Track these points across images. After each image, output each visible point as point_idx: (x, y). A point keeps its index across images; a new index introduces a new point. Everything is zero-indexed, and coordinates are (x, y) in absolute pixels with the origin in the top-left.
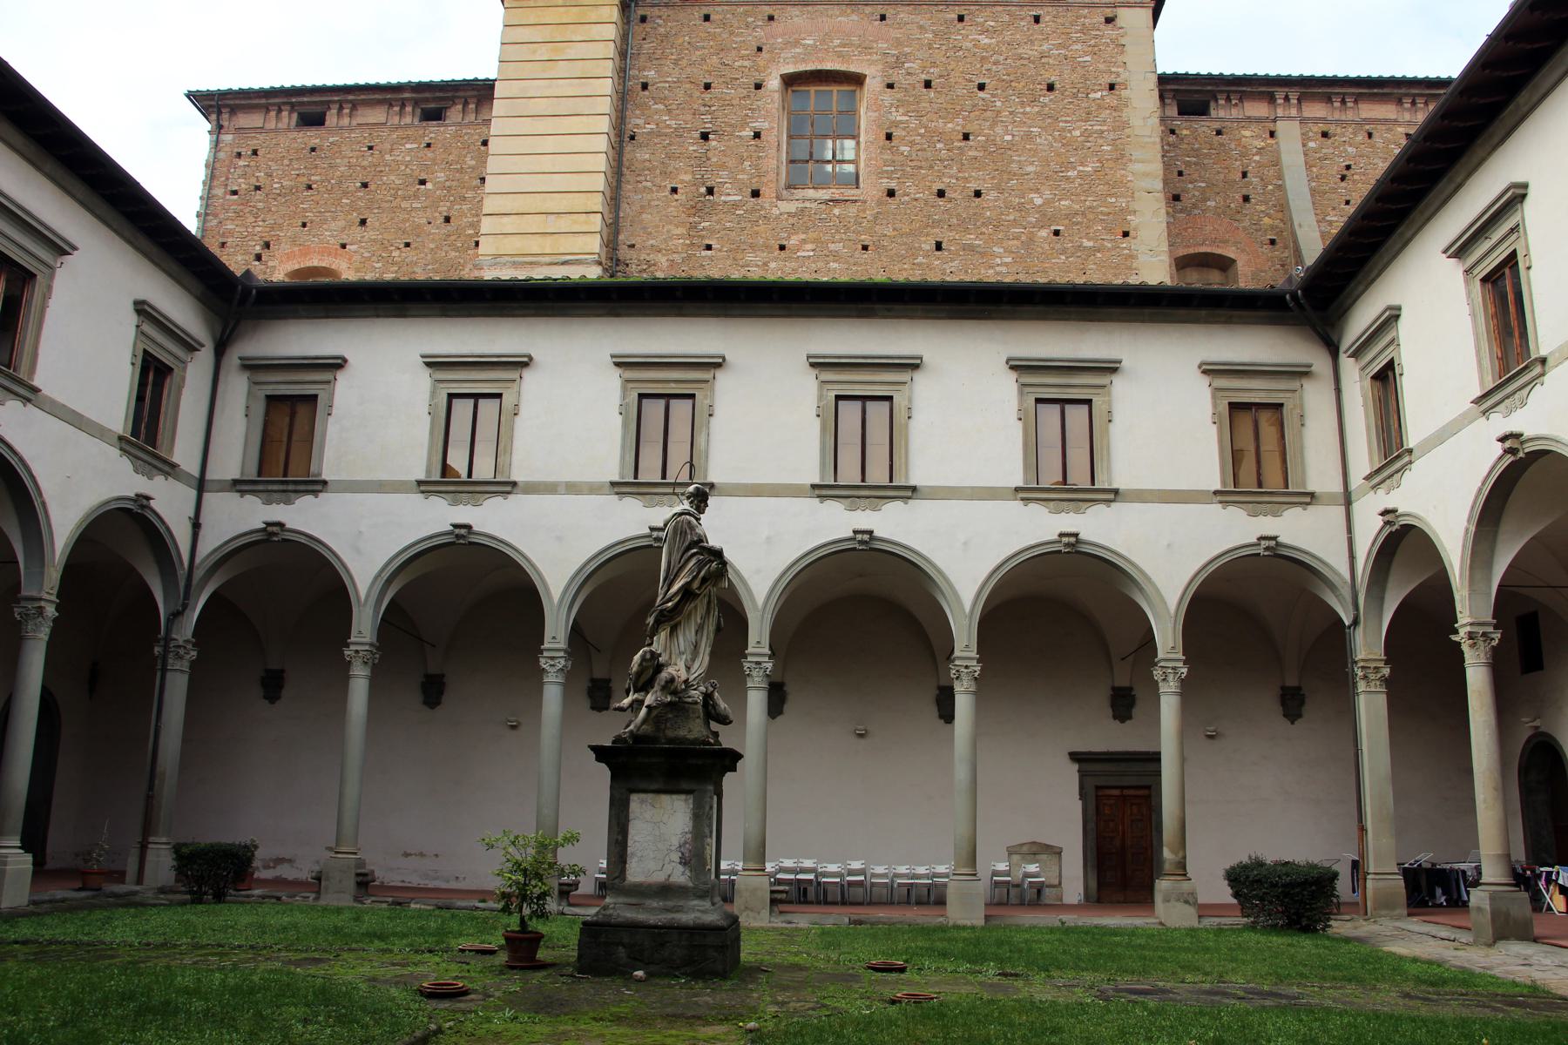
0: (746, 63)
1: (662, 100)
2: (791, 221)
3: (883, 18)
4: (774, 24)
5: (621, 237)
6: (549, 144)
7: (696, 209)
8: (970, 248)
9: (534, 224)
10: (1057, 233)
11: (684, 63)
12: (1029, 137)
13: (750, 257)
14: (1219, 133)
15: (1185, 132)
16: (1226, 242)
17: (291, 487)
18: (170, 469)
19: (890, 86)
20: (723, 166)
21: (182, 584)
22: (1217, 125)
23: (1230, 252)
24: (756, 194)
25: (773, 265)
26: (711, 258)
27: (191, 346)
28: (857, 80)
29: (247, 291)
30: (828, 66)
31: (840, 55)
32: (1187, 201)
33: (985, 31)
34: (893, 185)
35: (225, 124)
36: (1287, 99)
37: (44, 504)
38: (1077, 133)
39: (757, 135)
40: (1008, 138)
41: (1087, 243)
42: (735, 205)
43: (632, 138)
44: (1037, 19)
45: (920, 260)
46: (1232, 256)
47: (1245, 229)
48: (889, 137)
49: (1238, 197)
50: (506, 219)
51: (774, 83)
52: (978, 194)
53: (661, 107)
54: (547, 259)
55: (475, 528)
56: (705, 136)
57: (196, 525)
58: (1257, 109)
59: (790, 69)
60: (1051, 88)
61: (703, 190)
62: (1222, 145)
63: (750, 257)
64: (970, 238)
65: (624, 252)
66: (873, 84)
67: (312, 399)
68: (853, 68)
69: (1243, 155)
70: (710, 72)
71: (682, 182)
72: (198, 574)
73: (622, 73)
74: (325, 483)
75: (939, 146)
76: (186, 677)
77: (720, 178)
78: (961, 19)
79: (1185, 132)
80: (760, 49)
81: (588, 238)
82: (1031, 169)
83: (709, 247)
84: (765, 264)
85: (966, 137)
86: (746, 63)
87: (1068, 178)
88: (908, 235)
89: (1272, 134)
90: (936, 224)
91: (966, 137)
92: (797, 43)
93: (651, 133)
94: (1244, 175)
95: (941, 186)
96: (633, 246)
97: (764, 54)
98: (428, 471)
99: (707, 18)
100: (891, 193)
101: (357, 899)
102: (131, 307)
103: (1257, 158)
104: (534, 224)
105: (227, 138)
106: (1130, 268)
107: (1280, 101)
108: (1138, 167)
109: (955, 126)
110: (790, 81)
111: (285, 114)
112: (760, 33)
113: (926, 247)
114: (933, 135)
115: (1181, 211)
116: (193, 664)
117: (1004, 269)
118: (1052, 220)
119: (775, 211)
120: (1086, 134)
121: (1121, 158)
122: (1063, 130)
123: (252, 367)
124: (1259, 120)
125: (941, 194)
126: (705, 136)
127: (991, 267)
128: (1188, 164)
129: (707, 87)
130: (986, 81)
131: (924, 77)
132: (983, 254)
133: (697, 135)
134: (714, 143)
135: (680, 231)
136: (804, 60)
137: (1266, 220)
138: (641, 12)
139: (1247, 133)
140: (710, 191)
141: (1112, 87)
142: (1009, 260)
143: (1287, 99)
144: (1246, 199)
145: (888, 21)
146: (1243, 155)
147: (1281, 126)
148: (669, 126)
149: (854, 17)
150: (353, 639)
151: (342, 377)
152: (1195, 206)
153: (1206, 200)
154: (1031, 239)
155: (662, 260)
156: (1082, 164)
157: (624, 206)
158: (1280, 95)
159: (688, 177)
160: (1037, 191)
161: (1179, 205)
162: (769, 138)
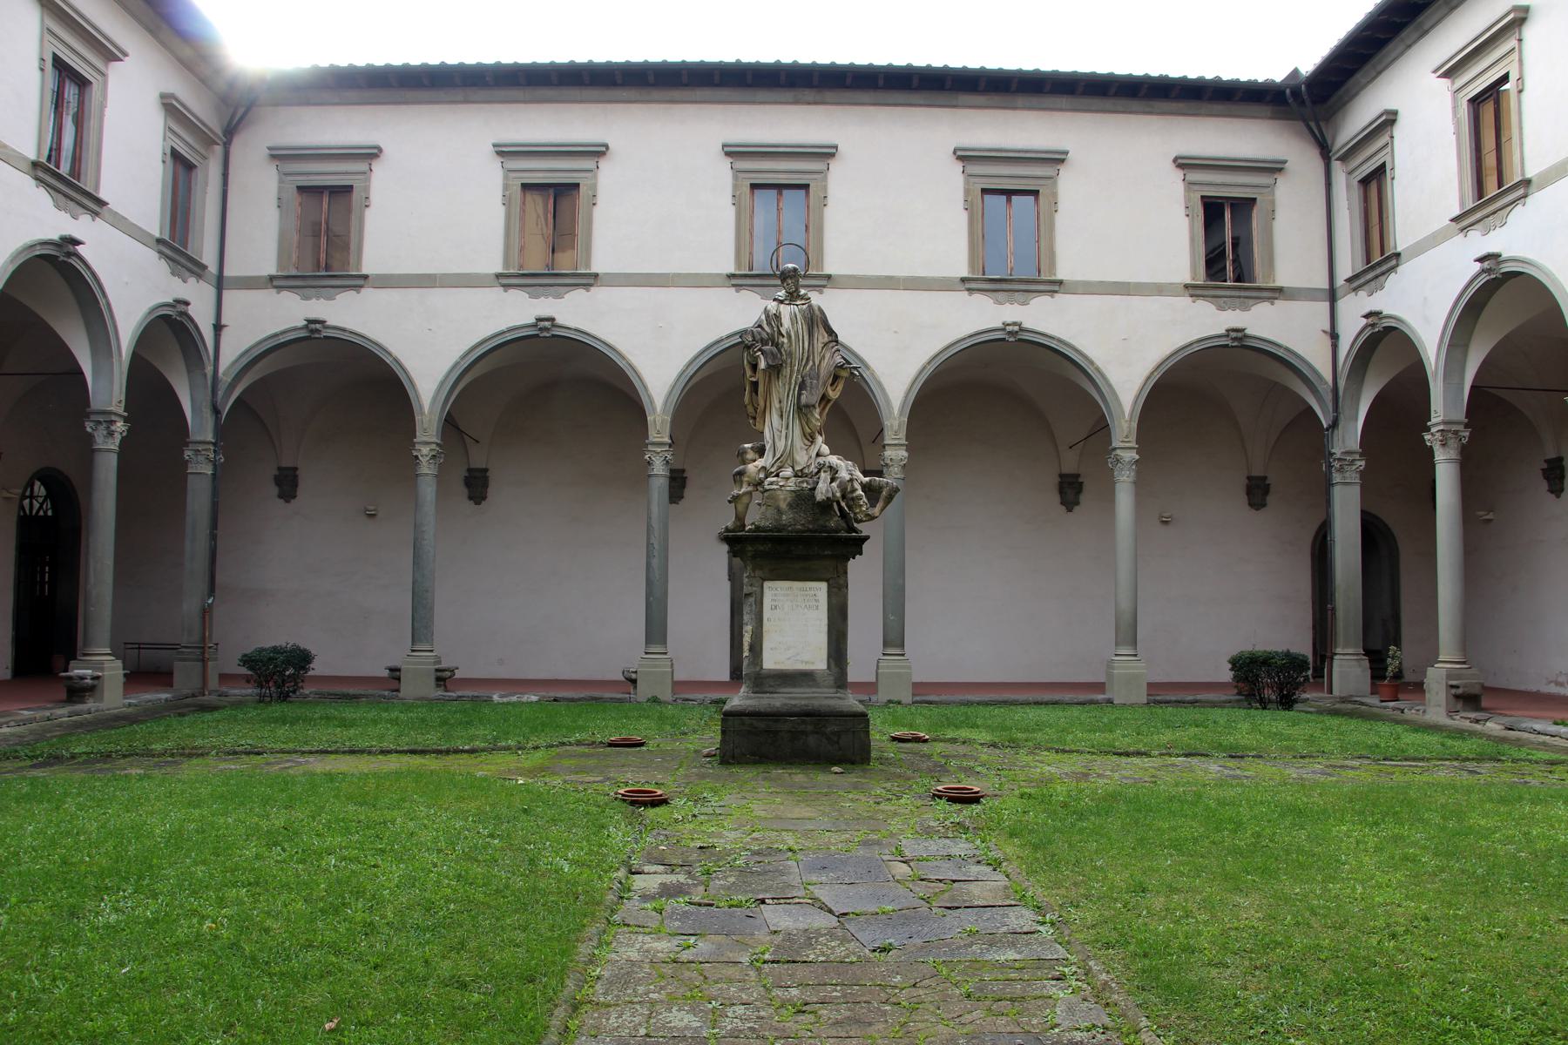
17: (1378, 271)
18: (1278, 293)
21: (1329, 398)
27: (1274, 168)
29: (1296, 92)
37: (1098, 369)
55: (1505, 255)
57: (1334, 336)
67: (1382, 169)
72: (1342, 383)
74: (1398, 255)
76: (1357, 489)
98: (1462, 203)
101: (1451, 713)
102: (1172, 167)
116: (1363, 474)
123: (1344, 158)
150: (1434, 421)
151: (1398, 131)
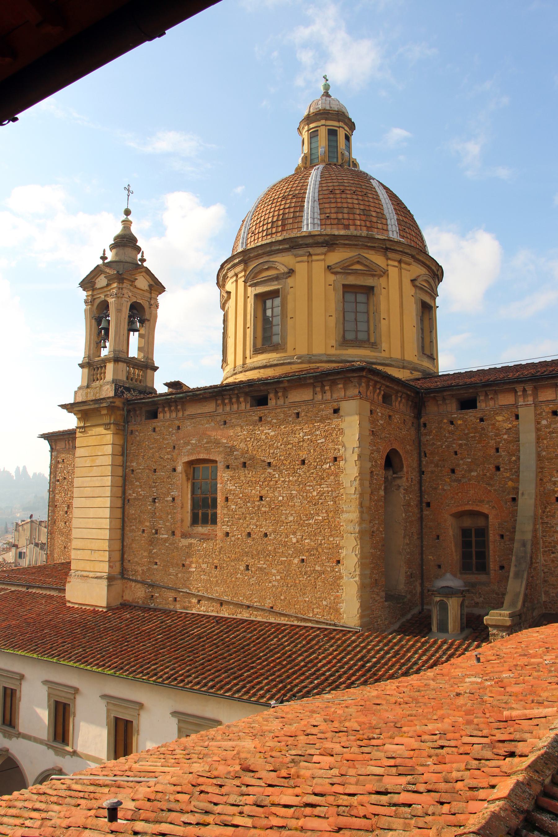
0: (169, 456)
1: (138, 480)
2: (186, 551)
3: (225, 423)
4: (180, 431)
5: (125, 556)
6: (91, 513)
7: (151, 542)
8: (261, 569)
9: (86, 555)
10: (303, 560)
11: (146, 457)
12: (292, 497)
13: (171, 570)
14: (482, 420)
15: (460, 422)
16: (482, 501)
19: (228, 467)
20: (161, 518)
22: (479, 415)
23: (485, 509)
24: (173, 533)
25: (180, 575)
26: (156, 569)
28: (216, 462)
30: (202, 456)
31: (206, 449)
32: (458, 474)
33: (273, 426)
34: (228, 529)
35: (54, 447)
36: (524, 390)
38: (315, 493)
39: (174, 499)
40: (281, 498)
41: (318, 568)
42: (166, 540)
43: (129, 500)
44: (298, 415)
45: (239, 576)
46: (486, 511)
47: (495, 490)
48: (227, 499)
49: (492, 467)
50: (79, 552)
51: (180, 468)
52: (266, 535)
53: (138, 483)
54: (91, 575)
56: (154, 500)
58: (506, 399)
59: (186, 459)
60: (303, 462)
61: (154, 531)
62: (483, 429)
63: (171, 570)
64: (261, 564)
65: (127, 565)
66: (221, 466)
68: (212, 458)
69: (496, 435)
70: (155, 462)
71: (146, 526)
73: (124, 466)
75: (249, 504)
77: (160, 525)
78: (260, 419)
79: (460, 422)
80: (174, 447)
81: (102, 564)
82: (291, 518)
83: (156, 564)
84: (177, 574)
85: (261, 498)
86: (169, 456)
87: (310, 524)
88: (233, 561)
89: (517, 417)
90: (247, 554)
91: (261, 498)
92: (188, 443)
93: (135, 499)
94: (497, 450)
95: (248, 530)
96: (129, 561)
97: (176, 451)
99: (154, 430)
100: (227, 534)
103: (505, 437)
104: (86, 555)
105: (53, 453)
106: (339, 585)
107: (520, 393)
108: (344, 516)
109: (255, 492)
110: (190, 463)
111: (70, 442)
112: (174, 438)
113: (242, 568)
114: (247, 499)
115: (455, 481)
117: (276, 583)
118: (301, 552)
119: (180, 545)
120: (321, 494)
121: (337, 511)
122: (309, 491)
124: (507, 407)
125: (249, 534)
126: (154, 500)
127: (270, 582)
128: (461, 445)
129: (155, 471)
130: (272, 461)
131: (242, 460)
132: (267, 574)
133: (151, 499)
134: (157, 504)
135: (145, 554)
136: (192, 454)
137: (510, 483)
138: (130, 429)
139: (500, 418)
140: (156, 533)
141: (335, 459)
142: (278, 577)
143: (524, 390)
144: (498, 468)
145: (227, 425)
146: (496, 435)
147: (521, 412)
148: (141, 495)
149: (213, 424)
152: (463, 476)
153: (471, 471)
154: (290, 563)
155: (140, 569)
156: (318, 514)
157: (126, 539)
158: (519, 388)
159: (148, 524)
160: (294, 533)
161: (454, 477)
162: (178, 501)
